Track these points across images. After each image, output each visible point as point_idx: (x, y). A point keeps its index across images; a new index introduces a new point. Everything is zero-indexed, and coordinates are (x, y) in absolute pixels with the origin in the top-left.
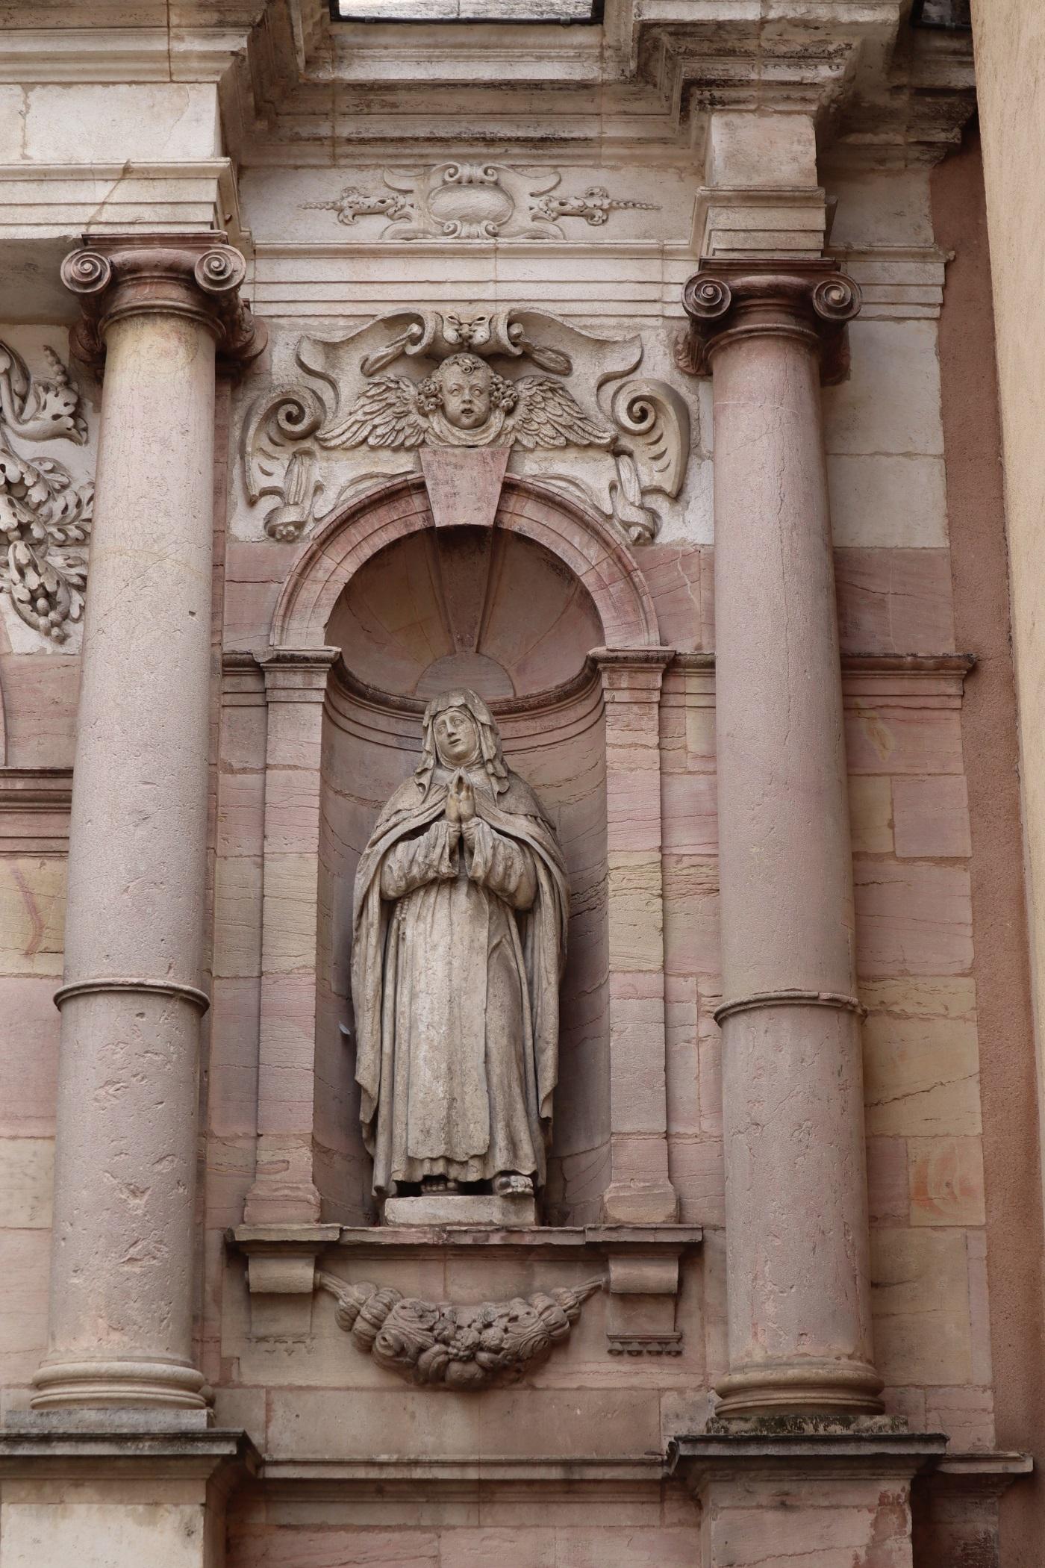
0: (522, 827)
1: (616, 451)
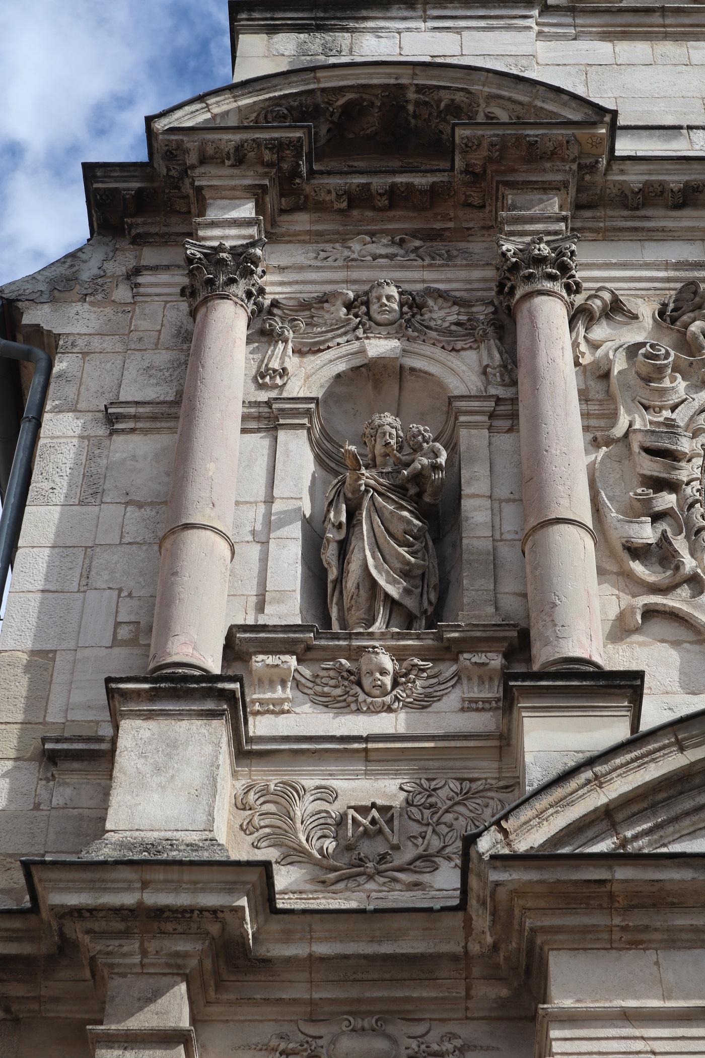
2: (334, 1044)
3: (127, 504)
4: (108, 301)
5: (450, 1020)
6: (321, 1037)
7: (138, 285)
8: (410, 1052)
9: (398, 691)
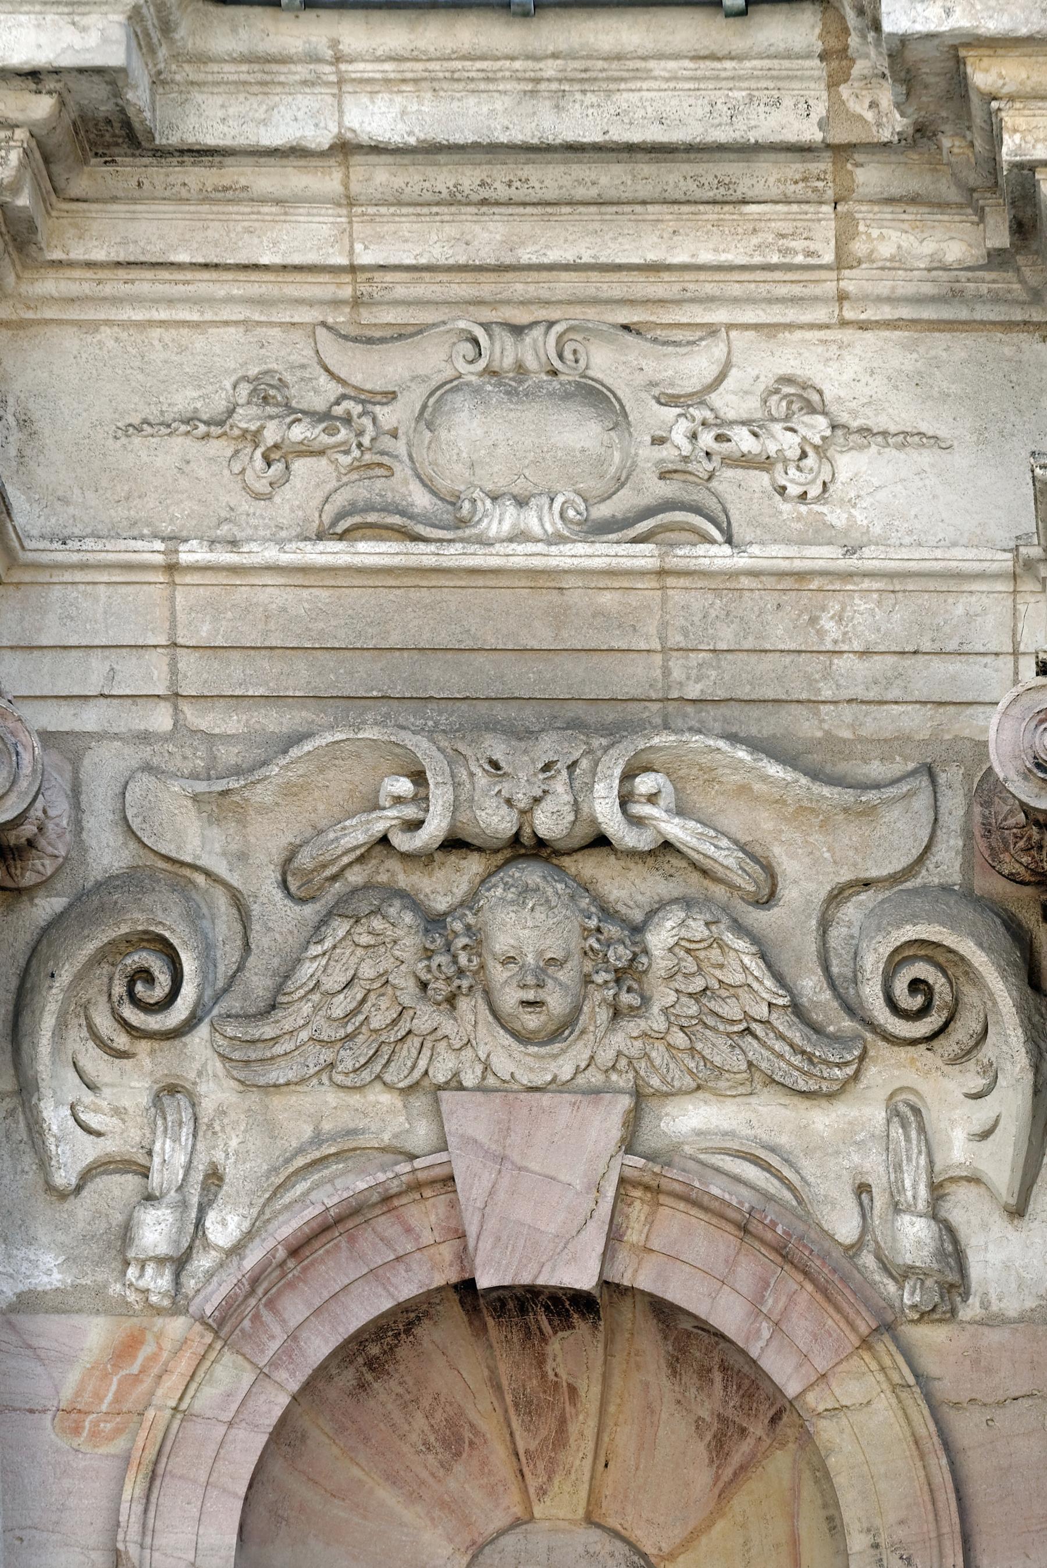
2: (430, 426)
5: (790, 327)
6: (390, 396)
8: (666, 452)
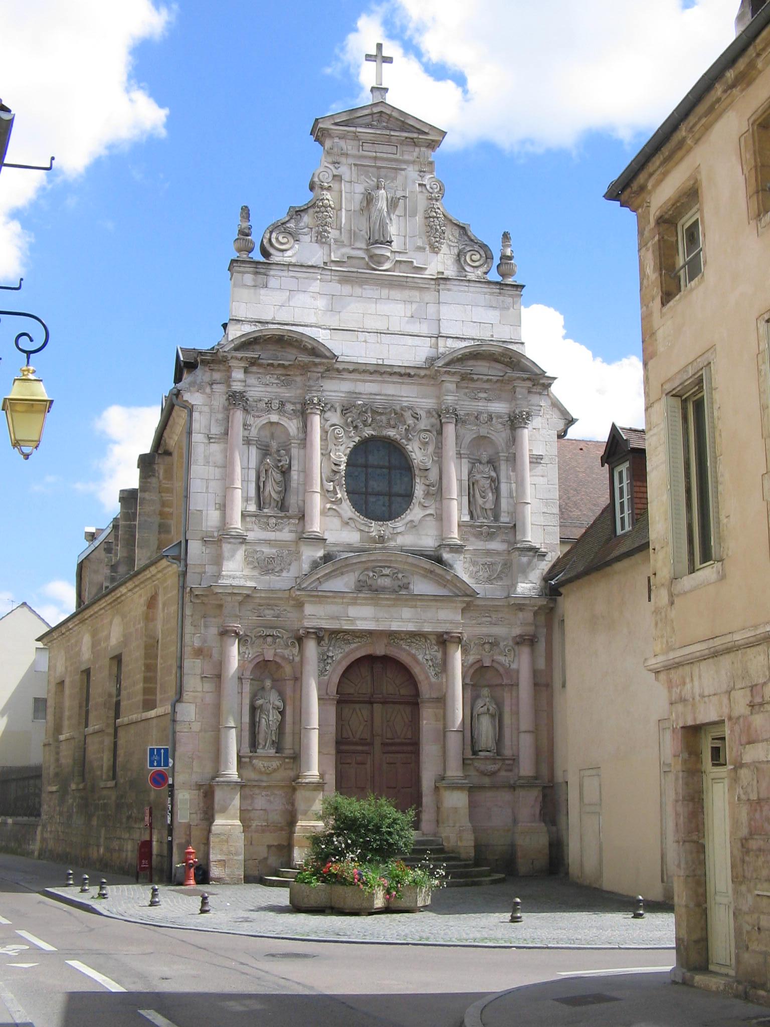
0: (494, 706)
1: (505, 655)
3: (215, 466)
4: (204, 393)
7: (212, 389)
9: (276, 527)
